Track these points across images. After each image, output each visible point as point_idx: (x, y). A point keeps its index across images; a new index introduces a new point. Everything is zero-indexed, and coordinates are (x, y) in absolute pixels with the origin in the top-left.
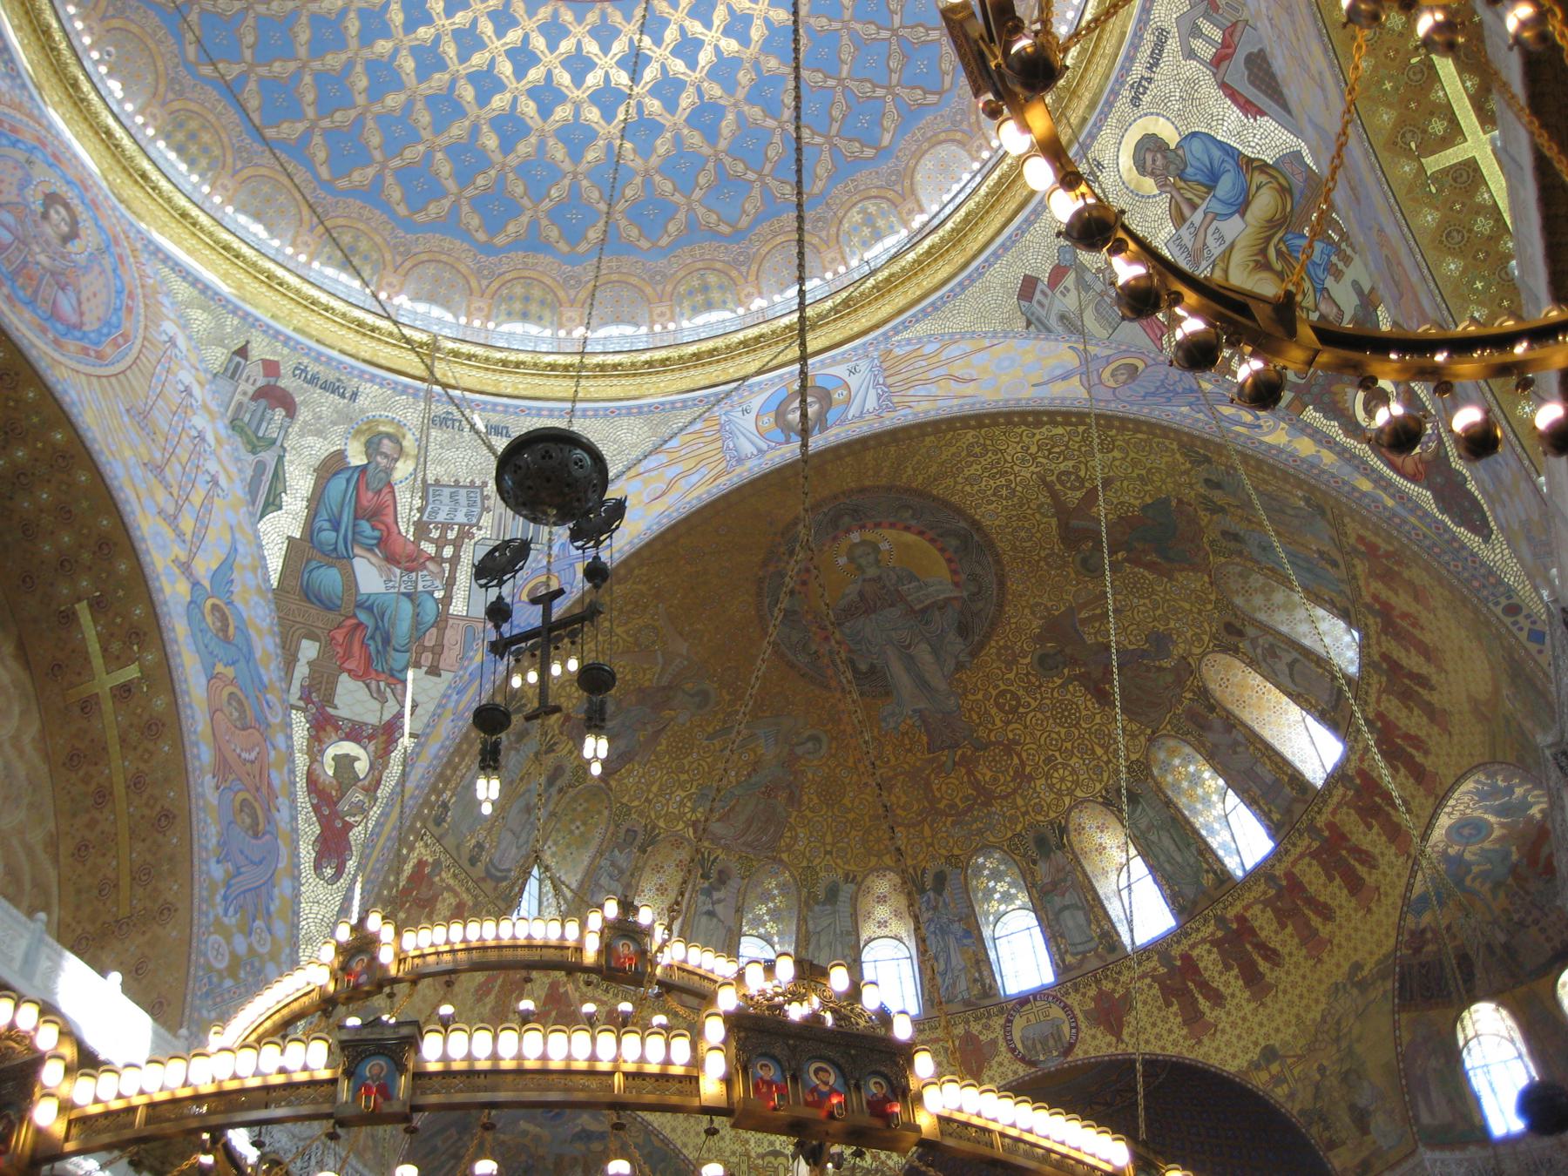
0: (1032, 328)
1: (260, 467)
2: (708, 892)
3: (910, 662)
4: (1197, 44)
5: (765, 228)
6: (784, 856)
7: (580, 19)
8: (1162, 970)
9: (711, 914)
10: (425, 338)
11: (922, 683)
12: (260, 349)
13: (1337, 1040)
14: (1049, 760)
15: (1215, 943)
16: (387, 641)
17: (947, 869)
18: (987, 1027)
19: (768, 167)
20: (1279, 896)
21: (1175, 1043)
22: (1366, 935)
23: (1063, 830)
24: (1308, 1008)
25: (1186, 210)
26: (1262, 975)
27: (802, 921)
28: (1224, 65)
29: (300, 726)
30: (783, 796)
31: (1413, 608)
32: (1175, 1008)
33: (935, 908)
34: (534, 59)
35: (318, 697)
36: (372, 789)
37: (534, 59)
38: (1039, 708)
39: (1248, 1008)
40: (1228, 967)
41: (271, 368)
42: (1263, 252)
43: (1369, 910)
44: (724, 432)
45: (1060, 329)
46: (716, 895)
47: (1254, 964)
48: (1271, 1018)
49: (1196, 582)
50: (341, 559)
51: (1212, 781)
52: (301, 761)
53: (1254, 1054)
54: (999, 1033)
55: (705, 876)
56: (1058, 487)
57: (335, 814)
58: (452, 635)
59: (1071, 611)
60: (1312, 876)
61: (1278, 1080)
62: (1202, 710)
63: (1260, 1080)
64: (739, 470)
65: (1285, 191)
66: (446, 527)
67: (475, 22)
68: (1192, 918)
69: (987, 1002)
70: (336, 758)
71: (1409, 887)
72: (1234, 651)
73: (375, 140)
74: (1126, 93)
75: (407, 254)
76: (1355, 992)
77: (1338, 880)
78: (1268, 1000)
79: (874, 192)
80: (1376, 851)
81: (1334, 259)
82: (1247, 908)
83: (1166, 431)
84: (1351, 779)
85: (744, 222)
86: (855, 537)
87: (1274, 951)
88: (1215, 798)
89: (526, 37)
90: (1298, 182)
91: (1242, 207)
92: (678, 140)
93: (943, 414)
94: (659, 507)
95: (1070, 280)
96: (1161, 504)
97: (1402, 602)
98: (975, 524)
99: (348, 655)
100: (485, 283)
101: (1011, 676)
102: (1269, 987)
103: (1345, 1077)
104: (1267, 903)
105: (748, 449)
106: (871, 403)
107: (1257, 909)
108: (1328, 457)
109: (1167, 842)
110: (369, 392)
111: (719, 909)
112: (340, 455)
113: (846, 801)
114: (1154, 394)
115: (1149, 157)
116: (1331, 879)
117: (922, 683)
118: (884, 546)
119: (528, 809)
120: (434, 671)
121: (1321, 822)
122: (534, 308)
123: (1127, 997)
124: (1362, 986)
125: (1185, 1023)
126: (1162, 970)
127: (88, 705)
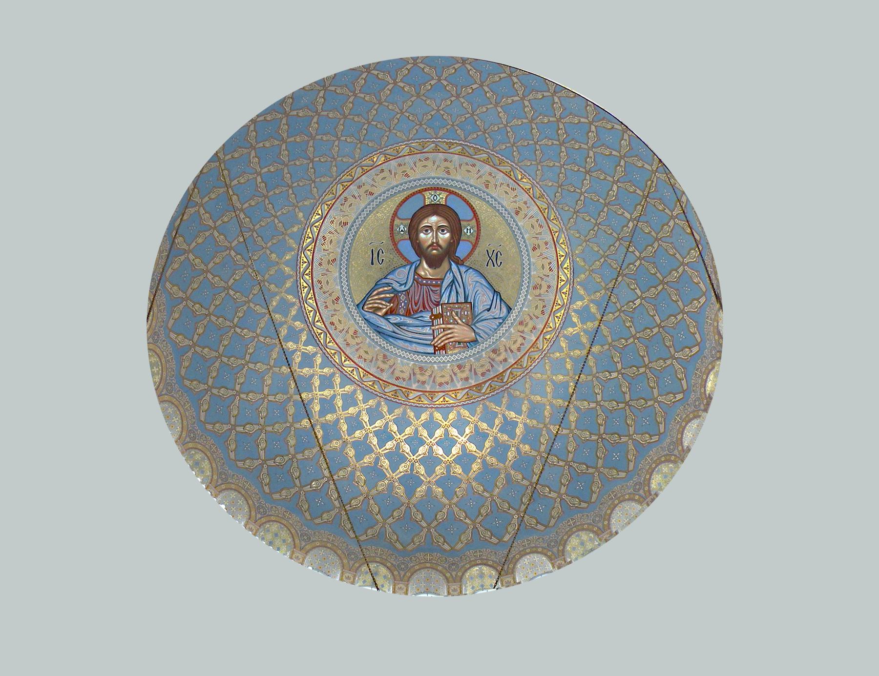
5: (420, 555)
7: (365, 401)
19: (435, 523)
34: (333, 410)
37: (333, 410)
67: (312, 376)
75: (225, 481)
79: (490, 563)
85: (410, 548)
89: (334, 396)
92: (391, 486)
100: (259, 516)
122: (278, 542)
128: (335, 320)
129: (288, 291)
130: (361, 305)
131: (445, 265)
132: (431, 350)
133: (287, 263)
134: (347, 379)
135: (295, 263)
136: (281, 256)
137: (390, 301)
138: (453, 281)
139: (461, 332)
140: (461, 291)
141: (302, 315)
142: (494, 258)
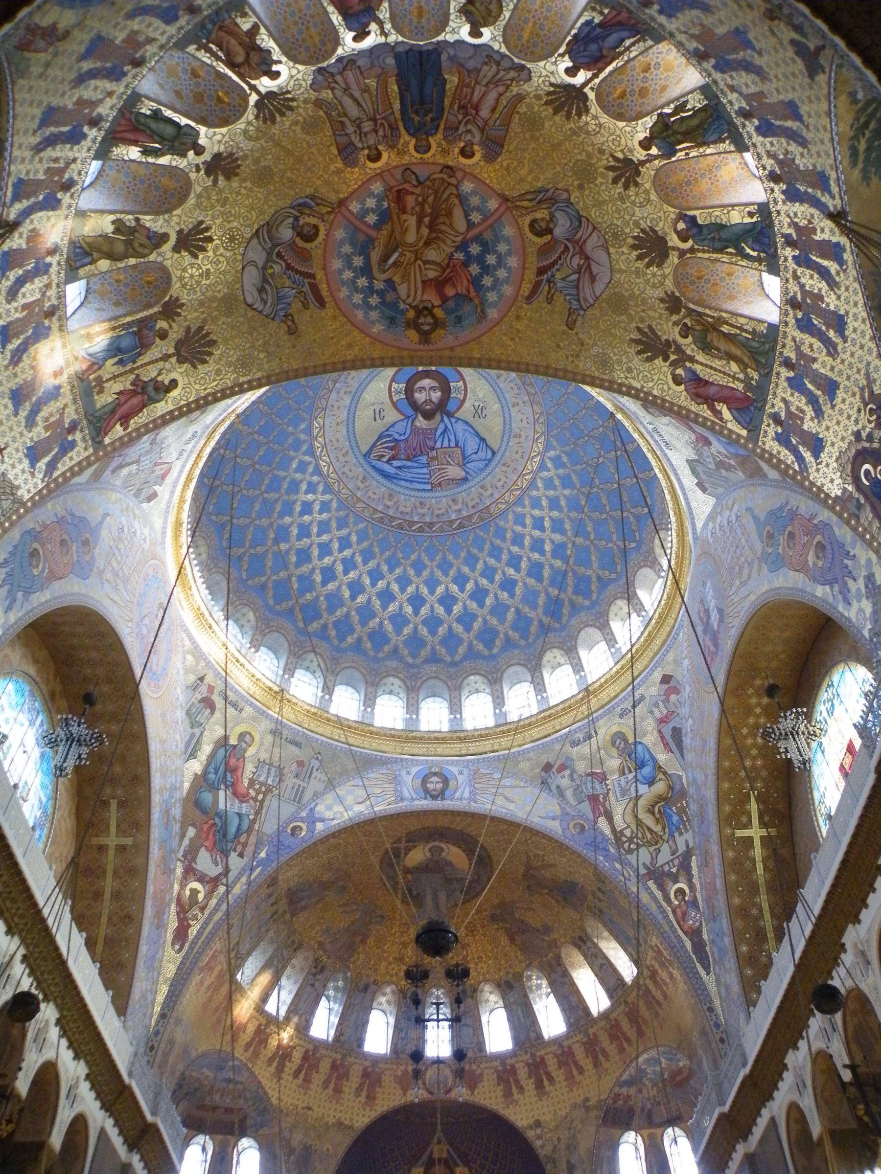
1: (193, 735)
2: (314, 975)
3: (435, 897)
4: (656, 710)
5: (427, 667)
9: (313, 985)
10: (276, 689)
11: (437, 907)
12: (209, 679)
14: (479, 957)
15: (528, 1065)
16: (225, 835)
22: (596, 1087)
23: (475, 990)
27: (349, 997)
29: (179, 871)
30: (359, 939)
35: (191, 855)
36: (202, 909)
38: (484, 935)
39: (534, 1099)
40: (530, 1077)
41: (211, 689)
42: (653, 806)
44: (395, 780)
49: (575, 915)
50: (214, 788)
51: (545, 988)
52: (176, 887)
53: (531, 1121)
57: (186, 919)
58: (253, 839)
59: (514, 902)
60: (580, 1053)
61: (539, 1137)
62: (554, 962)
63: (530, 1134)
65: (670, 788)
66: (262, 784)
70: (192, 890)
72: (579, 948)
73: (270, 564)
74: (618, 710)
83: (590, 864)
86: (437, 844)
90: (677, 787)
91: (651, 783)
95: (567, 773)
96: (572, 883)
97: (664, 975)
98: (490, 857)
99: (207, 839)
104: (555, 1056)
105: (406, 794)
106: (466, 795)
107: (550, 1056)
108: (654, 908)
110: (248, 710)
112: (226, 737)
117: (437, 907)
119: (260, 928)
120: (241, 855)
121: (591, 1031)
123: (482, 1074)
124: (588, 1109)
127: (102, 849)
128: (346, 470)
129: (305, 454)
130: (367, 455)
131: (438, 417)
132: (429, 487)
133: (302, 431)
134: (359, 519)
135: (309, 431)
136: (296, 426)
137: (392, 448)
138: (446, 430)
139: (454, 471)
140: (452, 437)
141: (318, 471)
142: (479, 412)
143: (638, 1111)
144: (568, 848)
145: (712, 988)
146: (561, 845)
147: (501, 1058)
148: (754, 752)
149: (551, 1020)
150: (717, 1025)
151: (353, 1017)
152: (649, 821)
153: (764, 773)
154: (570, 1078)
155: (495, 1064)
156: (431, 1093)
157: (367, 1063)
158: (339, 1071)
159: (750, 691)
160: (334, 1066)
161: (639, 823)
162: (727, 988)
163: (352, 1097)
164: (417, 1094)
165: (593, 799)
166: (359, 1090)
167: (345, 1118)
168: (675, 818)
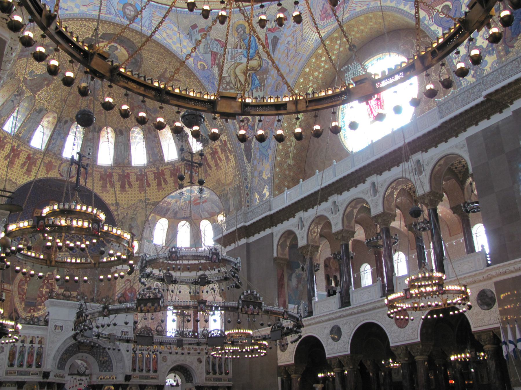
0: (188, 36)
6: (37, 96)
8: (103, 173)
9: (13, 101)
13: (135, 210)
15: (119, 175)
17: (69, 121)
18: (56, 162)
20: (140, 175)
21: (97, 190)
23: (100, 130)
24: (132, 200)
25: (238, 47)
26: (125, 188)
28: (270, 32)
31: (224, 158)
32: (101, 182)
33: (61, 128)
40: (119, 181)
43: (159, 191)
45: (194, 42)
46: (17, 97)
47: (125, 184)
48: (122, 197)
54: (58, 165)
55: (18, 92)
56: (168, 72)
60: (151, 177)
64: (109, 16)
65: (260, 65)
68: (117, 166)
69: (59, 156)
71: (171, 193)
76: (144, 204)
77: (156, 181)
78: (123, 193)
80: (169, 182)
81: (259, 87)
82: (131, 172)
84: (175, 166)
86: (115, 45)
87: (131, 185)
88: (136, 143)
90: (264, 67)
93: (162, 43)
94: (85, 9)
97: (223, 157)
101: (117, 91)
102: (126, 191)
103: (132, 218)
104: (136, 174)
105: (113, 11)
107: (133, 174)
109: (122, 147)
111: (15, 101)
113: (58, 92)
114: (206, 78)
115: (240, 29)
116: (155, 180)
118: (119, 50)
121: (161, 168)
124: (147, 204)
125: (102, 187)
126: (103, 173)
143: (171, 210)
144: (194, 75)
145: (249, 171)
146: (192, 72)
147: (105, 168)
148: (321, 70)
149: (139, 156)
150: (247, 187)
151: (30, 124)
152: (242, 78)
153: (320, 82)
154: (141, 188)
155: (100, 170)
156: (62, 176)
157: (31, 152)
158: (15, 153)
159: (338, 42)
160: (13, 149)
161: (236, 77)
162: (261, 173)
163: (19, 168)
164: (54, 174)
165: (214, 54)
166: (23, 165)
167: (13, 178)
168: (257, 82)
